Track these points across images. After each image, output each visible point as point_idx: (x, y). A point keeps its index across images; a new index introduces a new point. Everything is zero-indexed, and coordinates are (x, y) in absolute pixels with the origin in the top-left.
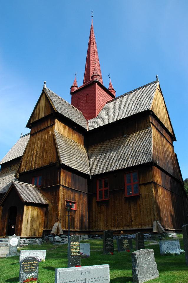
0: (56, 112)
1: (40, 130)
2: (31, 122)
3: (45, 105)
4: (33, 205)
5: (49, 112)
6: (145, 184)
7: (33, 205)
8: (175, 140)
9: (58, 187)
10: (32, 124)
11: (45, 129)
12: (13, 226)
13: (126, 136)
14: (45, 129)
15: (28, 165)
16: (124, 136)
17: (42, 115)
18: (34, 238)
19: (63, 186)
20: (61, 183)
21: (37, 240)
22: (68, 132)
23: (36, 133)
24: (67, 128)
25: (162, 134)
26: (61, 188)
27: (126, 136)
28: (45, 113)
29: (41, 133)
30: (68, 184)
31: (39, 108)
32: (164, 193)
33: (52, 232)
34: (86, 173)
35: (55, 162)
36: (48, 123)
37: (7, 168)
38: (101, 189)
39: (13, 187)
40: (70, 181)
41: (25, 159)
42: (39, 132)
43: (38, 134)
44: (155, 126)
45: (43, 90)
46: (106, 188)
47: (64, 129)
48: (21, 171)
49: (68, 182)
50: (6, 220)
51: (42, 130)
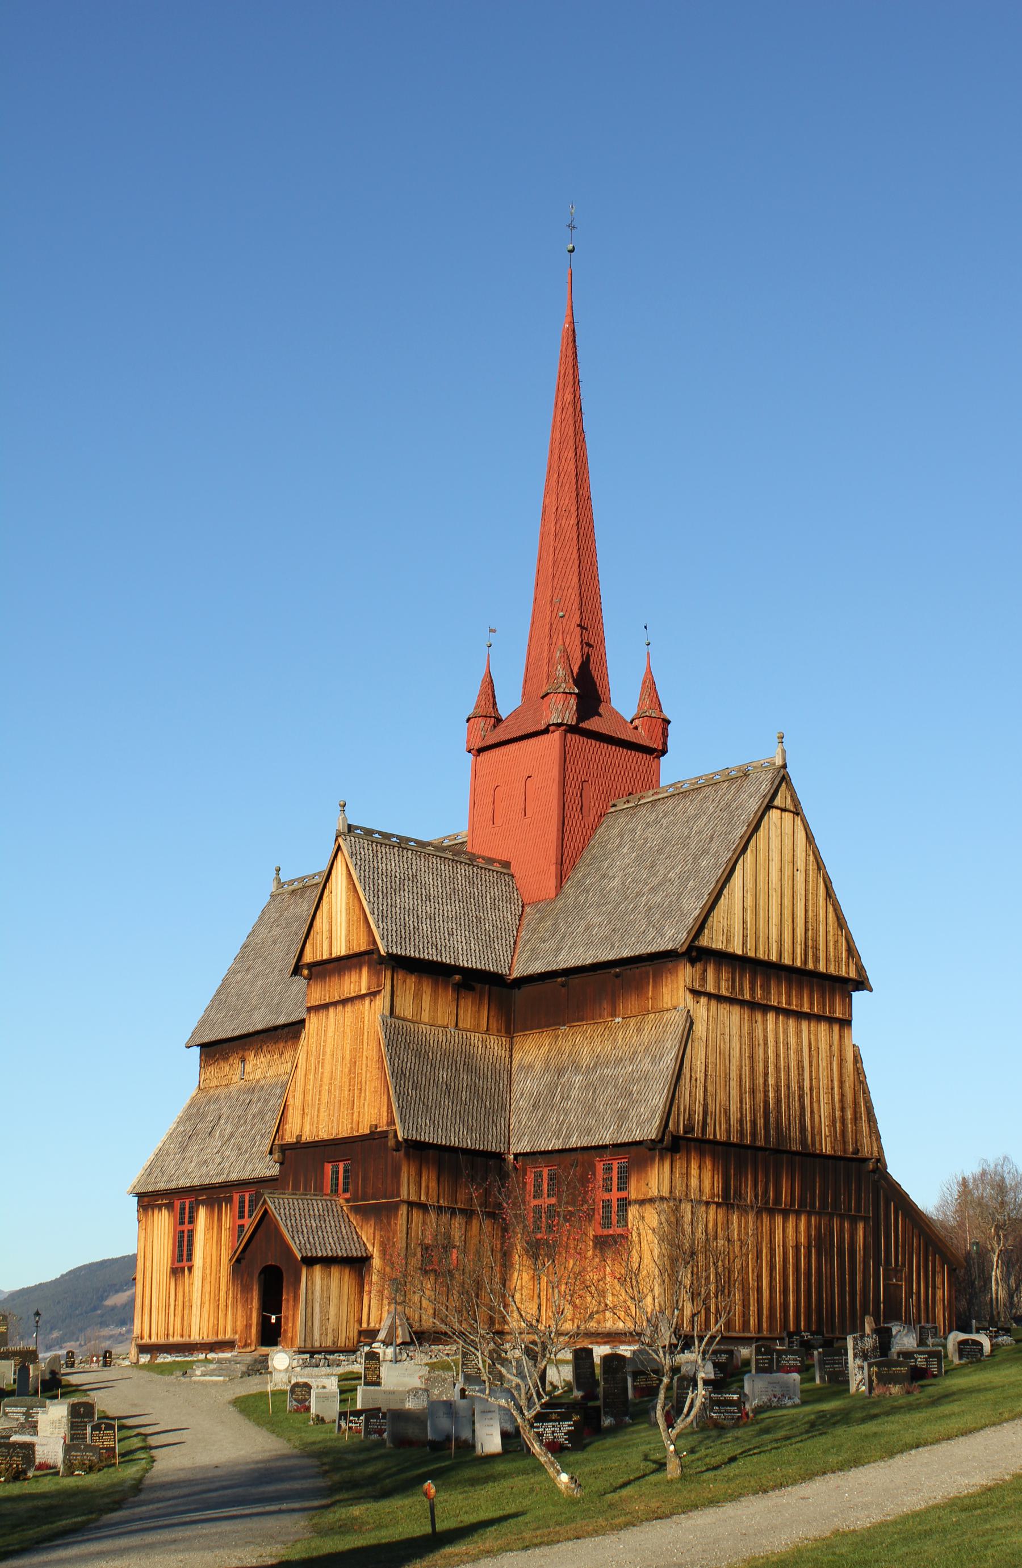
0: (382, 953)
1: (337, 998)
2: (308, 958)
3: (348, 909)
4: (328, 1261)
5: (361, 945)
6: (642, 1202)
7: (328, 1261)
8: (861, 983)
9: (396, 1207)
10: (310, 966)
11: (351, 1000)
12: (274, 1317)
13: (620, 1020)
14: (351, 1000)
15: (307, 1119)
16: (617, 1020)
17: (340, 949)
18: (332, 1353)
19: (411, 1204)
20: (404, 1195)
21: (342, 1358)
22: (435, 1000)
23: (325, 1007)
24: (429, 991)
25: (753, 1006)
26: (403, 1210)
27: (620, 1020)
28: (348, 941)
29: (340, 1008)
30: (427, 1194)
31: (330, 909)
32: (728, 1223)
33: (382, 1336)
34: (493, 1147)
35: (385, 1128)
36: (360, 977)
37: (231, 1060)
38: (537, 1202)
39: (266, 1210)
40: (433, 1184)
41: (297, 1094)
42: (335, 1004)
43: (331, 1010)
44: (710, 996)
45: (336, 839)
46: (553, 1200)
47: (418, 996)
48: (290, 1138)
49: (428, 1187)
50: (255, 1303)
51: (344, 1002)
